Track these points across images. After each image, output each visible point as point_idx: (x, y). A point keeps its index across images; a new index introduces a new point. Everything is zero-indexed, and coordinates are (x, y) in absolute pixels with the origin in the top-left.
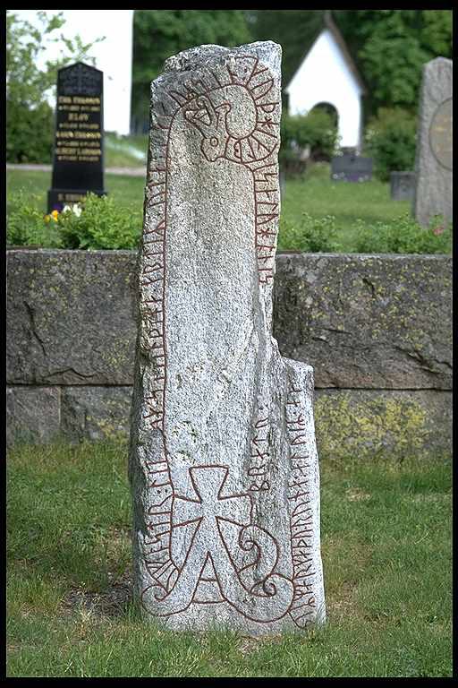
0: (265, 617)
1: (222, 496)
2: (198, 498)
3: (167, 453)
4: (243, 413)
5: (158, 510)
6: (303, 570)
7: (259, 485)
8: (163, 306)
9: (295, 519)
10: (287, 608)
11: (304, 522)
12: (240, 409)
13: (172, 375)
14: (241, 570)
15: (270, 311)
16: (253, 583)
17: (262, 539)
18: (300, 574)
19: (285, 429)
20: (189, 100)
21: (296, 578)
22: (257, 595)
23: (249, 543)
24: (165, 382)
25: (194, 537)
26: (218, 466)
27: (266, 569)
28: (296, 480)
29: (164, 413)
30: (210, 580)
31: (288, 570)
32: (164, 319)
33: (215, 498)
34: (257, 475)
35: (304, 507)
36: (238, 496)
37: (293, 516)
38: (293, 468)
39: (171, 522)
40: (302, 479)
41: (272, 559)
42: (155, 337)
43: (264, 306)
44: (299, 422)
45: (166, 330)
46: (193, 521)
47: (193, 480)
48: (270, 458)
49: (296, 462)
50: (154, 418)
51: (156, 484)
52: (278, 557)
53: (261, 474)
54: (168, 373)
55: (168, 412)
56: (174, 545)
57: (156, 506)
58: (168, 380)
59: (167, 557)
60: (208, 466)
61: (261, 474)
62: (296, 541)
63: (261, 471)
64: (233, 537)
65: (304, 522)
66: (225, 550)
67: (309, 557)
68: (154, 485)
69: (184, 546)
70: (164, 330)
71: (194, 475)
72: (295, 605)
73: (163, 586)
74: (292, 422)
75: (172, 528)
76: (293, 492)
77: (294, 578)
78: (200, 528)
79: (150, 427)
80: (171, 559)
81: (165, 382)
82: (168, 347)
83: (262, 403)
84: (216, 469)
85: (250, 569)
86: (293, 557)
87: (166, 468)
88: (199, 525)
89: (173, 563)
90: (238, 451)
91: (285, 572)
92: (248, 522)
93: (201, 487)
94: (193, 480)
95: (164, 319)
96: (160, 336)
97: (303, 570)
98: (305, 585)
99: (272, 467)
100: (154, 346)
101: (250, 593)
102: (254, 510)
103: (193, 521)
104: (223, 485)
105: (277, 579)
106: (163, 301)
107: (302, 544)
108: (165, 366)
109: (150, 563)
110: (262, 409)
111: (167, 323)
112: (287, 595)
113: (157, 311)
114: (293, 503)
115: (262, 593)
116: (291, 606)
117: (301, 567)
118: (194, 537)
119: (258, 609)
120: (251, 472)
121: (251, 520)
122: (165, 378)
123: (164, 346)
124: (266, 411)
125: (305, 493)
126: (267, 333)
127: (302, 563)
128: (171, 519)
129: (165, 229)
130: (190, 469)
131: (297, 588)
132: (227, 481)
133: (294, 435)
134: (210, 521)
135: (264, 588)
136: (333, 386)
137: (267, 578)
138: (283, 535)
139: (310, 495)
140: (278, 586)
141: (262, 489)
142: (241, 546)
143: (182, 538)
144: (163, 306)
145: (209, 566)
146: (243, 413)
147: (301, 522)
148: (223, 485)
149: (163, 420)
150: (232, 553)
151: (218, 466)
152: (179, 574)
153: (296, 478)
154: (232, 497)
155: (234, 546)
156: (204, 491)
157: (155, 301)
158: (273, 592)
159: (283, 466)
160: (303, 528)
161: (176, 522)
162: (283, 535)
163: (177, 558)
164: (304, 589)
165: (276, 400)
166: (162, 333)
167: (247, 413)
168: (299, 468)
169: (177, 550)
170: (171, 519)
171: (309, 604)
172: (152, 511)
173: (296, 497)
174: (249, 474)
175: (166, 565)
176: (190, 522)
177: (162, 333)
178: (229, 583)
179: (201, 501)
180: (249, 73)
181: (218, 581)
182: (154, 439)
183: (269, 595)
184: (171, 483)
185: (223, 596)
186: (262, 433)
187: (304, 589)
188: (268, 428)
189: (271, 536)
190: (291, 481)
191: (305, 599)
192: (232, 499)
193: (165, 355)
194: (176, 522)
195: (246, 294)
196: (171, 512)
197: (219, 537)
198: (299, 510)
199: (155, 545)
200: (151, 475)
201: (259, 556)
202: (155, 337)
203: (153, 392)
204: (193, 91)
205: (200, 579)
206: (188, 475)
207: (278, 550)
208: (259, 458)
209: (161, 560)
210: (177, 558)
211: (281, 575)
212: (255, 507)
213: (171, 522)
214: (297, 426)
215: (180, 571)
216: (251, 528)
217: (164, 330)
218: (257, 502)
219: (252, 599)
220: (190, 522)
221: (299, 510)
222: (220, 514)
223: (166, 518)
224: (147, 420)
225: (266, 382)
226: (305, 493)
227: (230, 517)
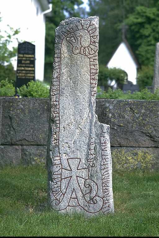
3: (60, 153)
5: (57, 173)
6: (106, 195)
8: (59, 103)
9: (103, 177)
11: (107, 178)
12: (85, 139)
15: (95, 105)
17: (92, 184)
24: (59, 129)
29: (59, 139)
30: (74, 198)
31: (101, 194)
39: (61, 178)
40: (106, 163)
41: (95, 191)
43: (93, 103)
45: (60, 111)
47: (68, 163)
49: (104, 157)
51: (56, 164)
52: (98, 190)
53: (92, 161)
55: (60, 139)
61: (92, 161)
63: (92, 160)
64: (82, 183)
68: (55, 165)
69: (65, 186)
72: (104, 207)
75: (61, 180)
76: (103, 167)
80: (61, 191)
82: (60, 117)
84: (76, 159)
85: (88, 195)
88: (71, 179)
93: (71, 166)
94: (68, 163)
96: (58, 113)
97: (106, 195)
98: (107, 200)
100: (56, 117)
101: (88, 203)
105: (97, 198)
107: (106, 185)
108: (59, 123)
109: (54, 192)
112: (101, 203)
113: (57, 105)
114: (103, 171)
115: (92, 203)
117: (106, 194)
119: (91, 208)
120: (88, 160)
122: (59, 128)
123: (59, 117)
126: (94, 113)
128: (61, 177)
129: (60, 77)
135: (93, 201)
136: (119, 146)
138: (99, 182)
139: (109, 168)
141: (92, 166)
144: (59, 103)
145: (74, 193)
147: (106, 178)
149: (58, 142)
153: (104, 163)
155: (82, 186)
156: (72, 167)
157: (56, 101)
158: (96, 202)
160: (106, 180)
161: (63, 177)
162: (99, 182)
163: (63, 190)
164: (107, 201)
168: (105, 159)
169: (63, 187)
170: (61, 177)
171: (108, 207)
173: (104, 169)
174: (88, 161)
179: (71, 170)
183: (95, 203)
184: (61, 164)
185: (79, 204)
186: (92, 147)
187: (107, 201)
189: (95, 183)
191: (107, 205)
193: (59, 120)
194: (63, 177)
195: (87, 99)
196: (61, 174)
197: (77, 183)
198: (105, 174)
200: (54, 161)
204: (69, 31)
205: (71, 198)
211: (99, 197)
212: (90, 172)
213: (61, 178)
221: (105, 174)
222: (78, 175)
227: (81, 176)
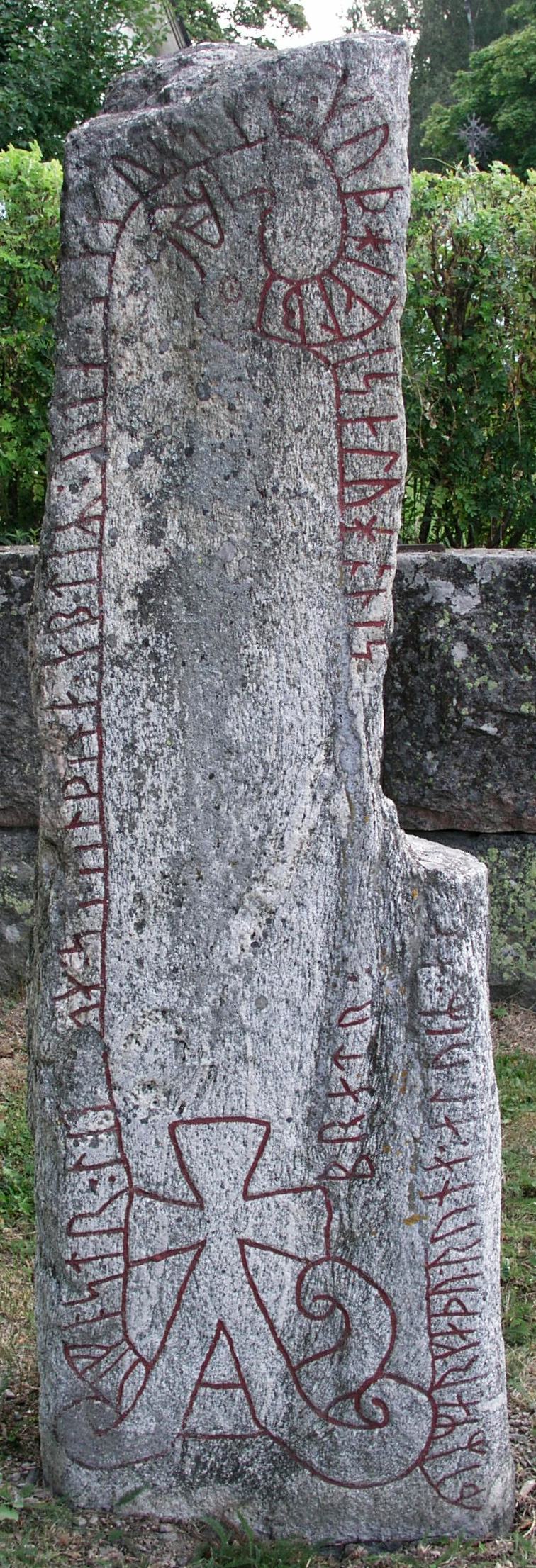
0: (358, 1477)
1: (253, 1189)
2: (192, 1198)
3: (111, 1087)
4: (308, 989)
5: (93, 1224)
6: (457, 1369)
7: (348, 1163)
8: (98, 719)
9: (438, 1248)
10: (414, 1456)
11: (462, 1255)
12: (300, 980)
13: (121, 894)
14: (301, 1364)
15: (379, 730)
16: (330, 1396)
17: (355, 1294)
18: (450, 1379)
19: (412, 1031)
20: (163, 178)
21: (439, 1386)
22: (341, 1424)
23: (320, 1302)
24: (107, 911)
25: (184, 1287)
26: (244, 1119)
27: (363, 1363)
28: (444, 1156)
29: (103, 988)
30: (224, 1386)
31: (420, 1365)
32: (101, 752)
33: (236, 1194)
34: (342, 1140)
35: (462, 1220)
36: (295, 1191)
37: (434, 1240)
38: (434, 1125)
39: (126, 1254)
40: (455, 1152)
41: (378, 1341)
42: (77, 797)
43: (361, 718)
44: (451, 1010)
45: (107, 781)
46: (183, 1250)
47: (179, 1154)
48: (372, 1100)
49: (441, 1111)
50: (78, 999)
51: (86, 1162)
52: (394, 1338)
53: (353, 1140)
54: (113, 888)
55: (113, 986)
56: (133, 1307)
57: (85, 1215)
58: (113, 906)
59: (119, 1336)
60: (218, 1120)
61: (353, 1140)
62: (440, 1301)
63: (354, 1131)
64: (282, 1287)
65: (462, 1255)
66: (261, 1317)
67: (472, 1337)
68: (79, 1167)
69: (156, 1310)
70: (100, 780)
71: (182, 1140)
72: (436, 1450)
73: (106, 1401)
74: (435, 1013)
75: (128, 1265)
76: (432, 1182)
77: (435, 1386)
78: (199, 1268)
79: (70, 1022)
80: (126, 1338)
81: (107, 911)
82: (113, 825)
83: (358, 966)
84: (237, 1126)
85: (323, 1364)
86: (432, 1336)
87: (112, 1123)
88: (196, 1260)
89: (133, 1347)
90: (295, 1083)
91: (411, 1372)
92: (321, 1252)
93: (199, 1169)
94: (179, 1154)
95: (101, 752)
96: (90, 794)
97: (457, 1369)
98: (461, 1404)
99: (377, 1121)
100: (76, 822)
101: (325, 1417)
102: (335, 1224)
103: (183, 1250)
104: (255, 1165)
105: (391, 1387)
106: (96, 704)
107: (455, 1307)
108: (105, 870)
109: (74, 1347)
110: (355, 978)
111: (108, 763)
112: (418, 1428)
113: (81, 732)
114: (435, 1210)
115: (354, 1418)
116: (425, 1451)
117: (452, 1361)
118: (184, 1287)
119: (345, 1457)
120: (328, 1133)
121: (328, 1247)
122: (107, 899)
123: (102, 821)
124: (366, 987)
125: (465, 1186)
126: (373, 788)
127: (453, 1351)
128: (126, 1247)
129: (101, 518)
130: (172, 1128)
131: (442, 1411)
132: (267, 1155)
133: (438, 1043)
134: (222, 1250)
135: (358, 1408)
136: (510, 829)
137: (367, 1384)
138: (408, 1287)
139: (480, 1190)
140: (395, 1407)
141: (353, 1175)
142: (308, 1315)
143: (154, 1291)
144: (98, 719)
145: (223, 1353)
146: (308, 989)
147: (454, 1255)
148: (255, 1165)
149: (101, 1005)
150: (279, 1324)
151: (244, 1119)
152: (148, 1373)
153: (442, 1149)
154: (278, 1192)
155: (283, 1309)
156: (207, 1180)
157: (75, 704)
158: (380, 1416)
159: (406, 1119)
160: (456, 1270)
161: (138, 1252)
162: (408, 1287)
163: (141, 1336)
164: (460, 1414)
165: (394, 959)
166: (95, 787)
167: (319, 989)
168: (449, 1123)
169: (140, 1320)
170: (126, 1247)
171: (470, 1446)
172: (77, 1227)
173: (441, 1196)
174: (321, 1138)
175: (112, 1357)
176: (174, 1252)
177: (95, 787)
178: (270, 1394)
179: (200, 1203)
180: (323, 107)
181: (244, 1386)
182: (80, 1052)
183: (372, 1425)
184: (123, 1161)
185: (257, 1422)
186: (358, 1039)
187: (460, 1414)
188: (370, 1026)
189: (376, 1286)
190: (429, 1156)
191: (460, 1437)
192: (280, 1197)
193: (106, 846)
194: (138, 1252)
195: (313, 687)
196: (125, 1230)
197: (247, 1287)
198: (449, 1226)
199: (86, 1308)
200: (71, 1142)
201: (347, 1332)
202: (77, 797)
203: (77, 938)
204: (174, 154)
205: (200, 1383)
206: (167, 1141)
207: (394, 1322)
208: (350, 1099)
209: (104, 1342)
210: (141, 1336)
211: (401, 1380)
212: (336, 1216)
213: (126, 1254)
214: (444, 1022)
215: (150, 1366)
216: (326, 1266)
217: (100, 780)
218: (343, 1205)
219: (329, 1433)
220: (174, 1252)
221: (449, 1226)
222: (248, 1234)
223: (114, 1244)
224: (61, 1006)
225: (366, 914)
226: (465, 1186)
227: (273, 1241)
